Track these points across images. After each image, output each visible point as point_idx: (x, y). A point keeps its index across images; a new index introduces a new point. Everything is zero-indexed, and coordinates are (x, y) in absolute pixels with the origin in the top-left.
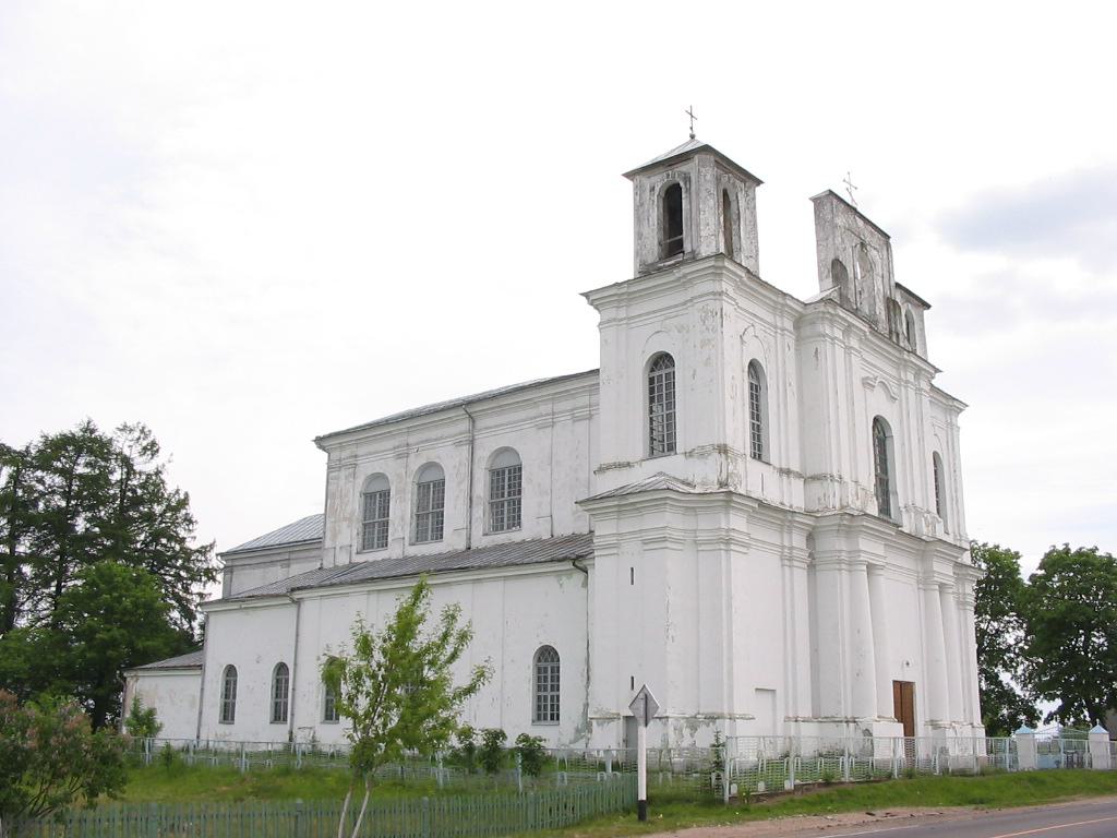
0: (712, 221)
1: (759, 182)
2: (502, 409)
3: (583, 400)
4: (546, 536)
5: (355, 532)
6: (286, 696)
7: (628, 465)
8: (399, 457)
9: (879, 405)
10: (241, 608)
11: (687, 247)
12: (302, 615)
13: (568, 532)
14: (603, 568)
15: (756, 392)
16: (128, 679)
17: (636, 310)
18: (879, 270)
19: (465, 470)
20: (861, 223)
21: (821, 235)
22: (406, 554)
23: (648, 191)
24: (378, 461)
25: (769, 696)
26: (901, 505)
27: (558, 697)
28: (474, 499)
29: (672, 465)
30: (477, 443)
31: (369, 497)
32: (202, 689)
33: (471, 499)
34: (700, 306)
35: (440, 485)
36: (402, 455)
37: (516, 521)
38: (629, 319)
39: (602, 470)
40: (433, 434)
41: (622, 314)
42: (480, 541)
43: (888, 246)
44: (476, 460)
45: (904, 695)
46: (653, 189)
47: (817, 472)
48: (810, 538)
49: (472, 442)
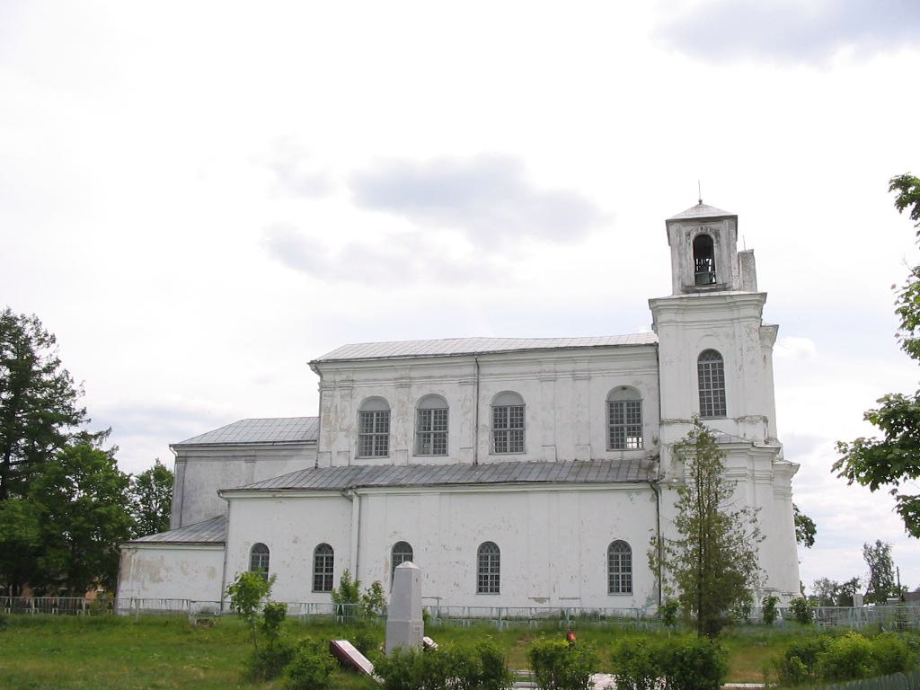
2: (506, 363)
5: (353, 442)
8: (401, 386)
10: (274, 497)
11: (719, 280)
12: (363, 505)
13: (571, 459)
16: (123, 551)
17: (690, 317)
22: (410, 463)
23: (684, 235)
27: (630, 577)
28: (480, 427)
31: (366, 416)
32: (225, 563)
34: (745, 324)
35: (442, 415)
36: (404, 384)
37: (519, 445)
38: (684, 323)
41: (679, 318)
42: (486, 456)
44: (480, 398)
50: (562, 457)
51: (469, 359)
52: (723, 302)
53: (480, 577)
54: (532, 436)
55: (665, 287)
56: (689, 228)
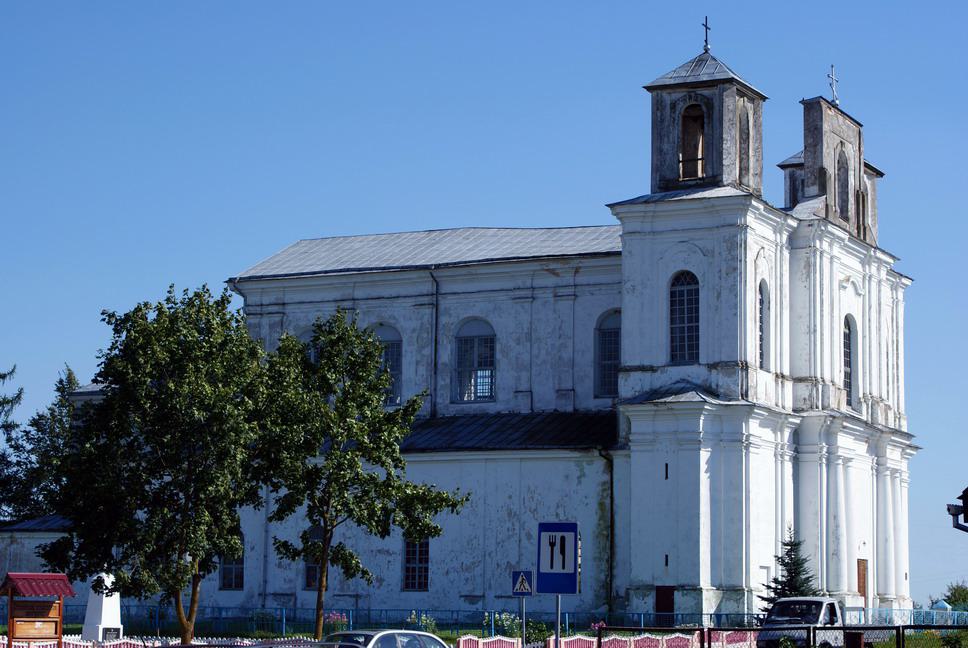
0: (733, 150)
4: (525, 410)
7: (652, 369)
9: (849, 303)
13: (551, 407)
21: (810, 141)
23: (668, 107)
25: (765, 571)
26: (861, 395)
28: (440, 367)
29: (694, 372)
30: (442, 307)
33: (436, 364)
44: (440, 326)
46: (673, 106)
49: (436, 306)
50: (539, 406)
51: (426, 273)
52: (701, 205)
53: (407, 569)
55: (641, 184)
56: (678, 95)
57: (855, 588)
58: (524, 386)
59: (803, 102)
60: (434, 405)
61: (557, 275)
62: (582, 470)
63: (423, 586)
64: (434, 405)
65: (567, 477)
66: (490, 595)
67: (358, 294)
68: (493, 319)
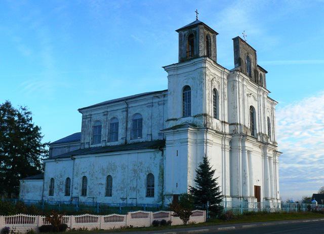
0: (203, 45)
1: (217, 34)
2: (136, 101)
3: (162, 99)
6: (70, 188)
7: (176, 119)
8: (104, 115)
9: (251, 102)
14: (169, 150)
15: (216, 98)
17: (180, 72)
18: (252, 61)
19: (125, 120)
20: (247, 46)
24: (98, 116)
27: (154, 189)
29: (189, 119)
30: (129, 112)
35: (117, 124)
36: (106, 114)
37: (141, 135)
39: (168, 120)
40: (115, 108)
41: (175, 73)
42: (130, 141)
43: (255, 54)
45: (257, 189)
46: (185, 35)
47: (233, 122)
48: (231, 142)
49: (127, 111)
54: (145, 131)
57: (253, 195)
58: (150, 133)
59: (233, 39)
60: (126, 140)
61: (159, 98)
62: (155, 156)
63: (111, 195)
64: (126, 140)
65: (151, 158)
66: (128, 198)
67: (109, 110)
68: (142, 113)
